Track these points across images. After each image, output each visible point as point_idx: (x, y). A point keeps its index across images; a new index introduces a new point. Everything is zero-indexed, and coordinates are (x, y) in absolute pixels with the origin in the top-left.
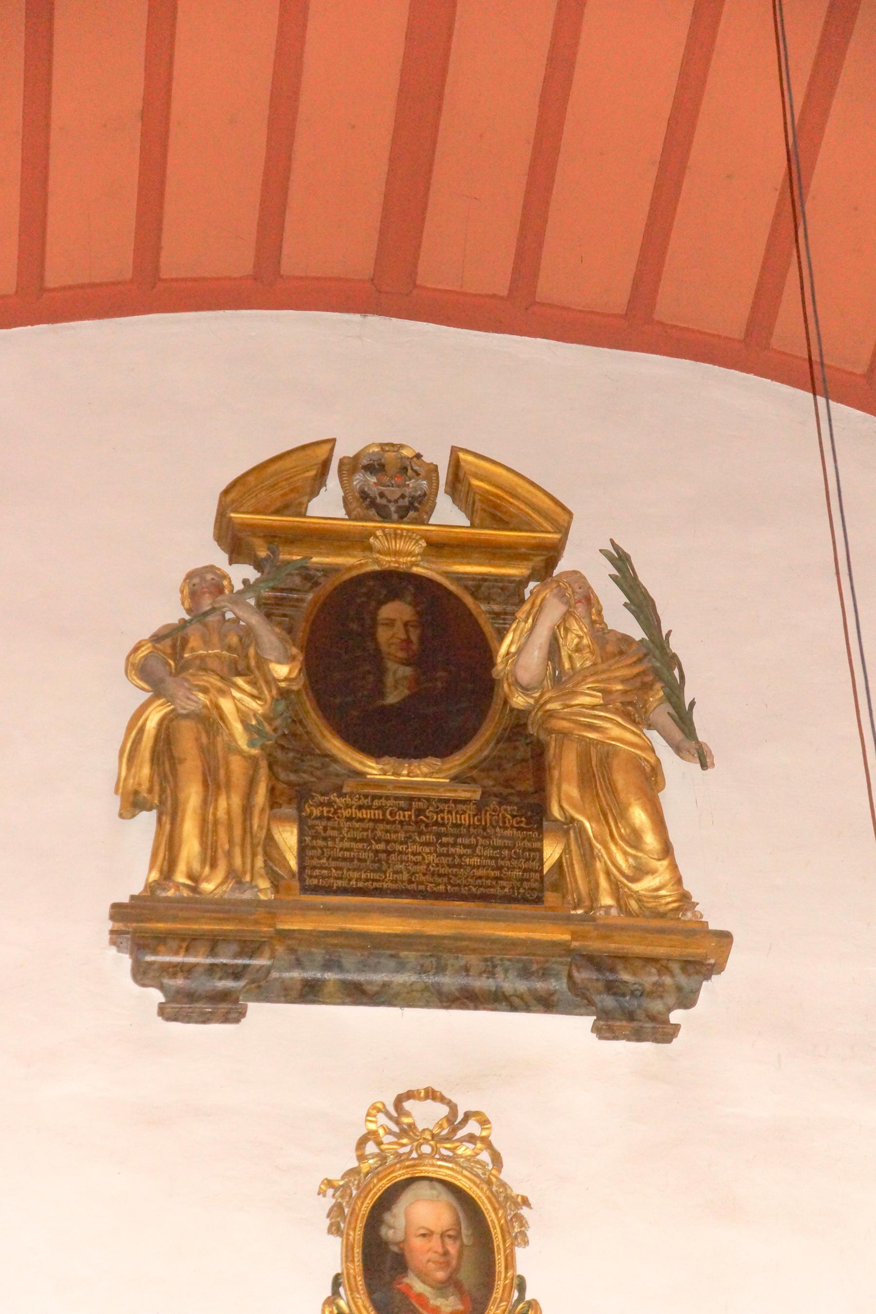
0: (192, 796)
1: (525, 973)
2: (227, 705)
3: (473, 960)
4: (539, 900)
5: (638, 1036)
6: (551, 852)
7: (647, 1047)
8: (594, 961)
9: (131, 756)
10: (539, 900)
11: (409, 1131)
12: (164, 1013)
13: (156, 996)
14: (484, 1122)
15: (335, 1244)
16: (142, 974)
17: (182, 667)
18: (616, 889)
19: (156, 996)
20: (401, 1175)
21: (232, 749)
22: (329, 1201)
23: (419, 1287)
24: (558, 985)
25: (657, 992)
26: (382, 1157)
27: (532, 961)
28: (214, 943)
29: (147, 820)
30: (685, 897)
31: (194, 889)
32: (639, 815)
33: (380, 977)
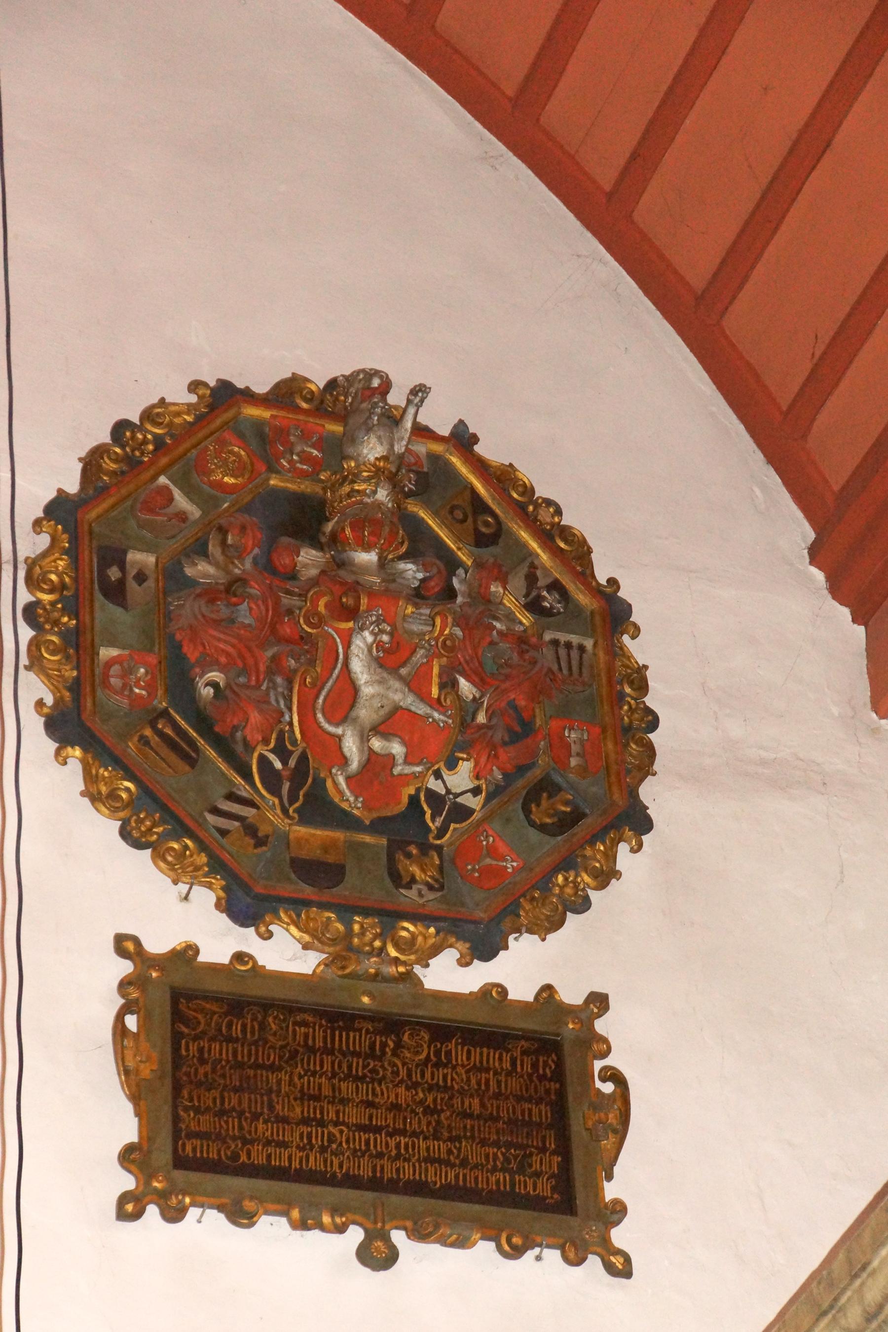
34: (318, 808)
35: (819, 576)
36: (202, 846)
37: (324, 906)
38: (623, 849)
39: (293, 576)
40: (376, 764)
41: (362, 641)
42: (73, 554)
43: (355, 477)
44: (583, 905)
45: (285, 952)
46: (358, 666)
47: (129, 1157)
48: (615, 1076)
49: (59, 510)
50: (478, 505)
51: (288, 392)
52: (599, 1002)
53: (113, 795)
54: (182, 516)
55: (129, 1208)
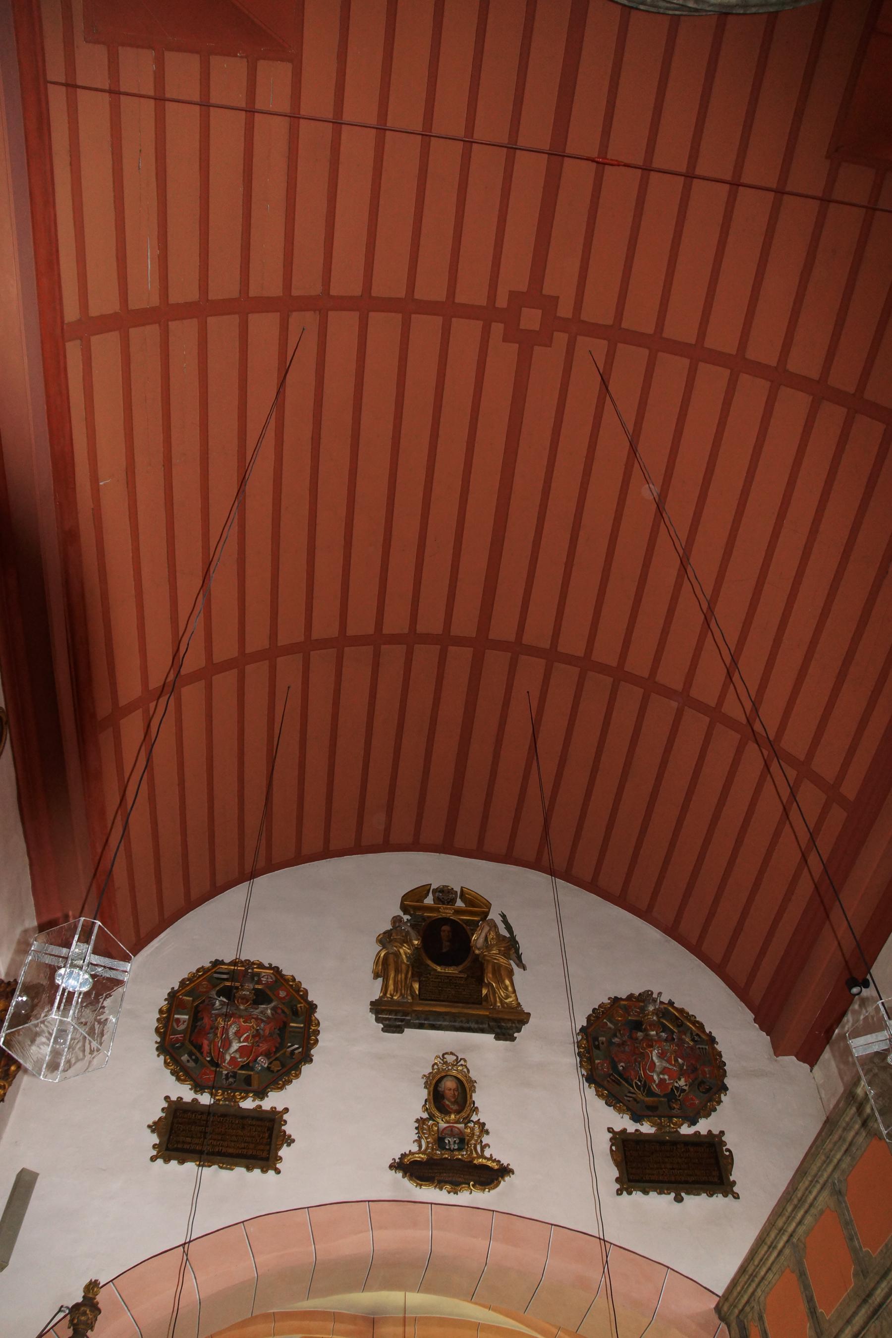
0: (392, 975)
1: (477, 1023)
2: (401, 951)
3: (464, 1019)
4: (481, 1004)
5: (506, 1040)
6: (484, 991)
7: (508, 1042)
8: (495, 1020)
9: (376, 963)
10: (481, 1004)
11: (446, 1063)
12: (383, 1030)
13: (382, 1026)
14: (465, 1061)
15: (426, 1091)
16: (378, 1020)
17: (390, 941)
18: (501, 1001)
19: (382, 1026)
20: (443, 1074)
21: (402, 962)
22: (424, 1080)
23: (447, 1103)
24: (486, 1026)
25: (511, 1028)
26: (438, 1069)
27: (479, 1020)
28: (396, 1012)
29: (380, 980)
30: (519, 1004)
31: (392, 998)
32: (507, 982)
33: (439, 1023)
34: (650, 1093)
35: (757, 1026)
36: (624, 1105)
37: (654, 1116)
38: (722, 1095)
39: (637, 1039)
40: (662, 1081)
41: (655, 1052)
42: (587, 1039)
43: (648, 1015)
44: (715, 1110)
45: (647, 1128)
46: (654, 1058)
47: (617, 1180)
48: (728, 1150)
49: (583, 1029)
50: (677, 1018)
51: (630, 997)
52: (722, 1133)
53: (603, 1094)
54: (610, 1028)
55: (619, 1192)
